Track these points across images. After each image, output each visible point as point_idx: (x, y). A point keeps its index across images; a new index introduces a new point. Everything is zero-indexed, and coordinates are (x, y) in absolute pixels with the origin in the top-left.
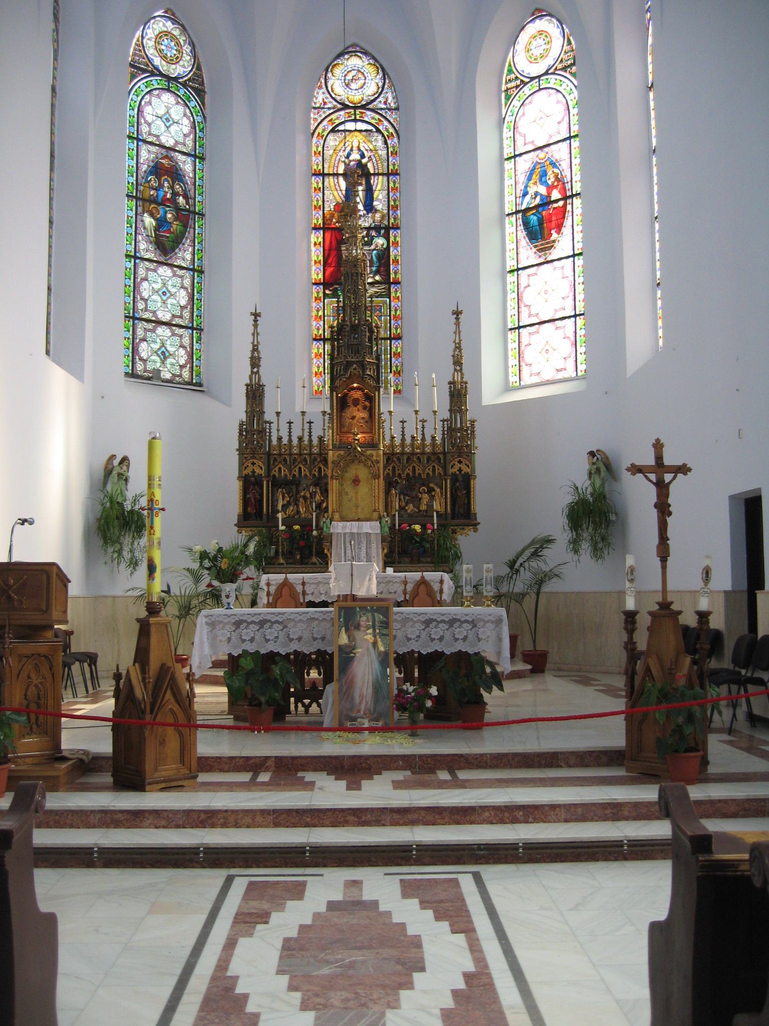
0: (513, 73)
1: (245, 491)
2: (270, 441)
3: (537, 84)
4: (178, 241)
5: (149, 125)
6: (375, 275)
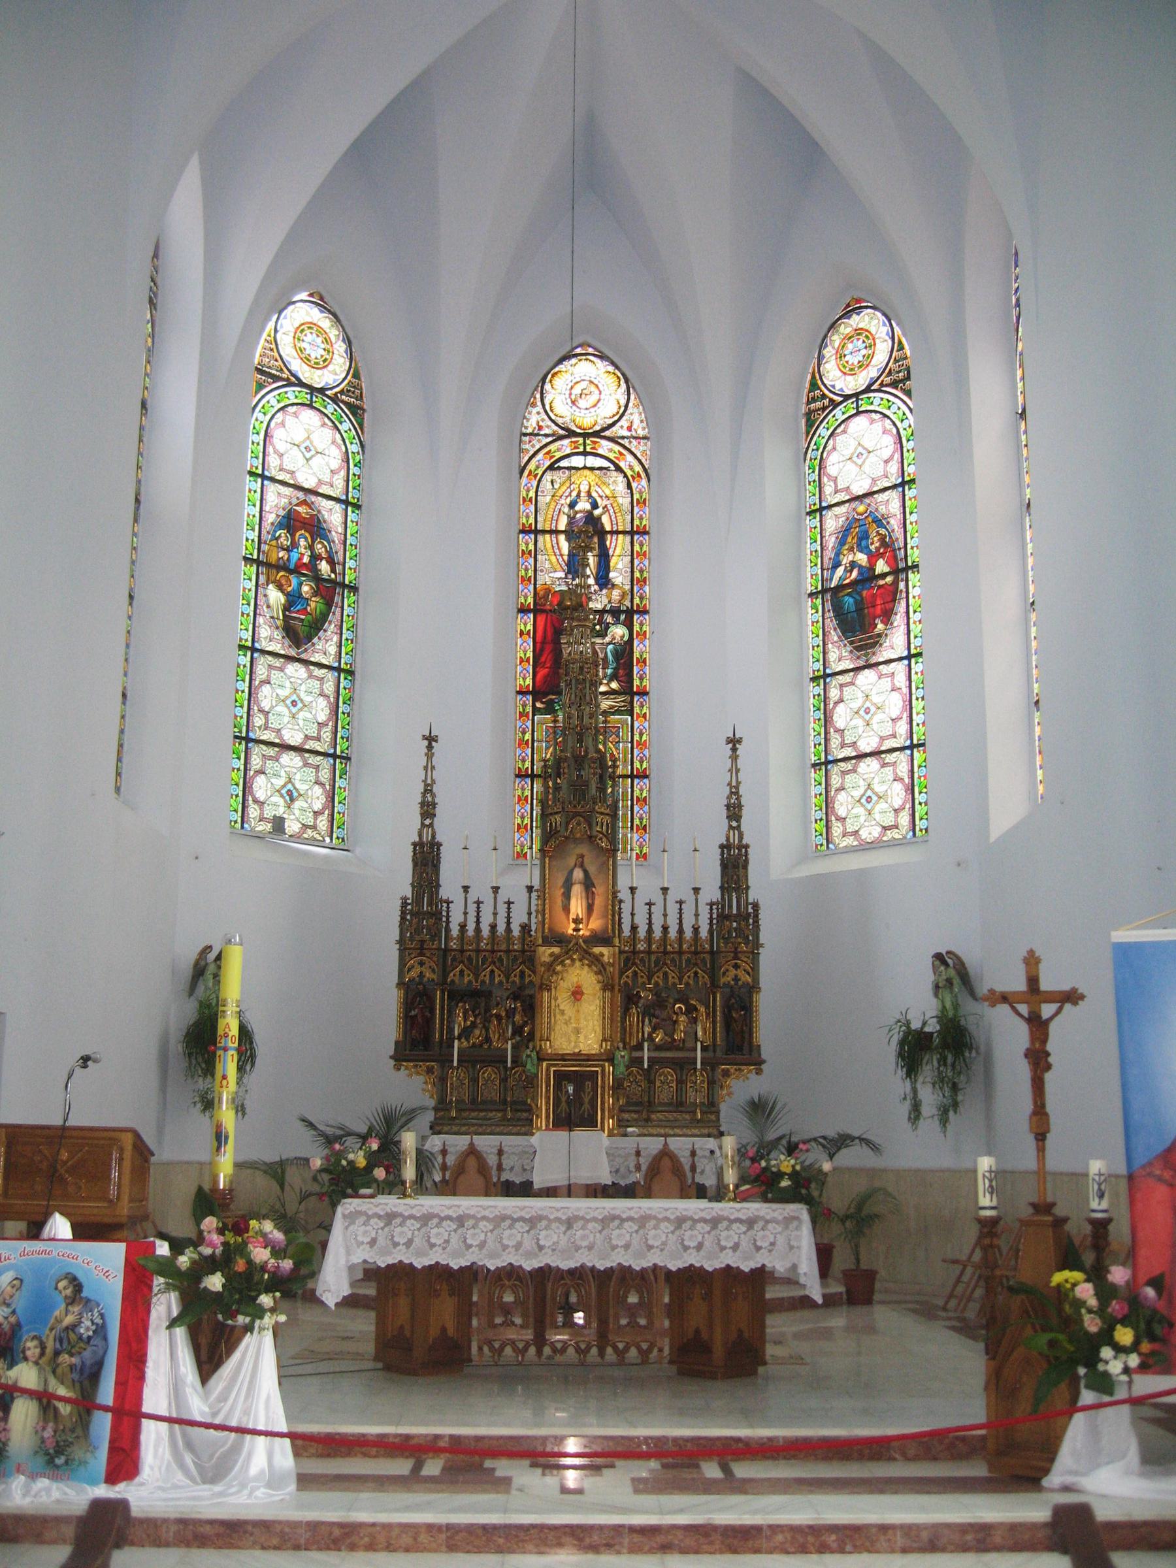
0: (819, 388)
1: (408, 1004)
3: (854, 405)
4: (317, 625)
5: (281, 456)
6: (611, 680)
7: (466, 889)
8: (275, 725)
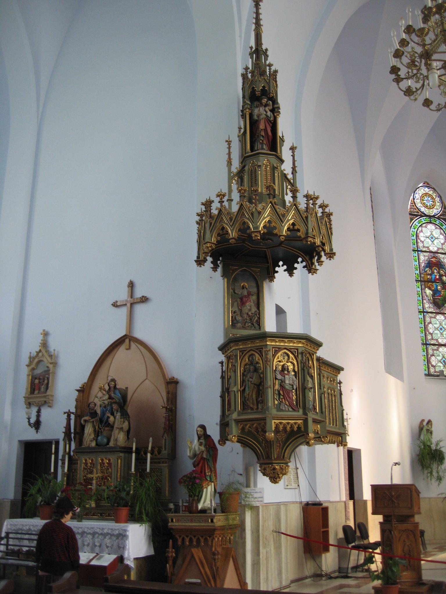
5: (423, 242)
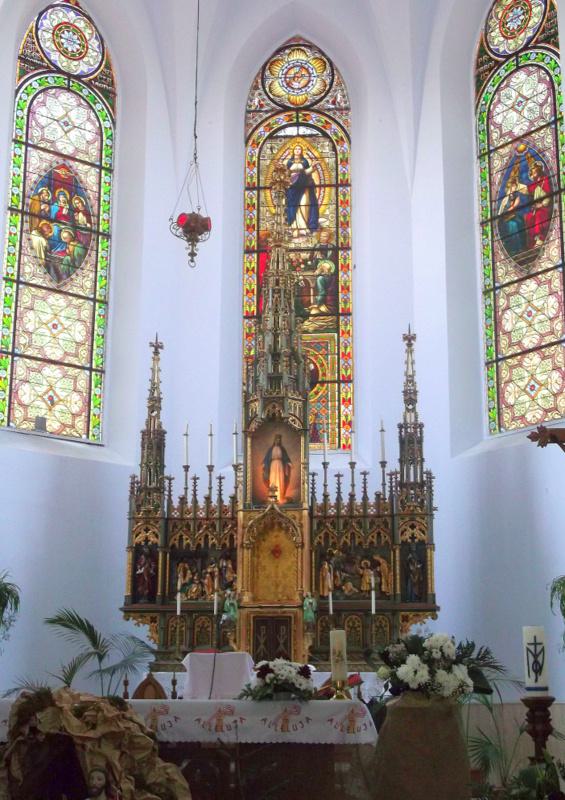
2: (170, 502)
4: (75, 265)
6: (320, 305)
7: (186, 468)
8: (39, 344)
